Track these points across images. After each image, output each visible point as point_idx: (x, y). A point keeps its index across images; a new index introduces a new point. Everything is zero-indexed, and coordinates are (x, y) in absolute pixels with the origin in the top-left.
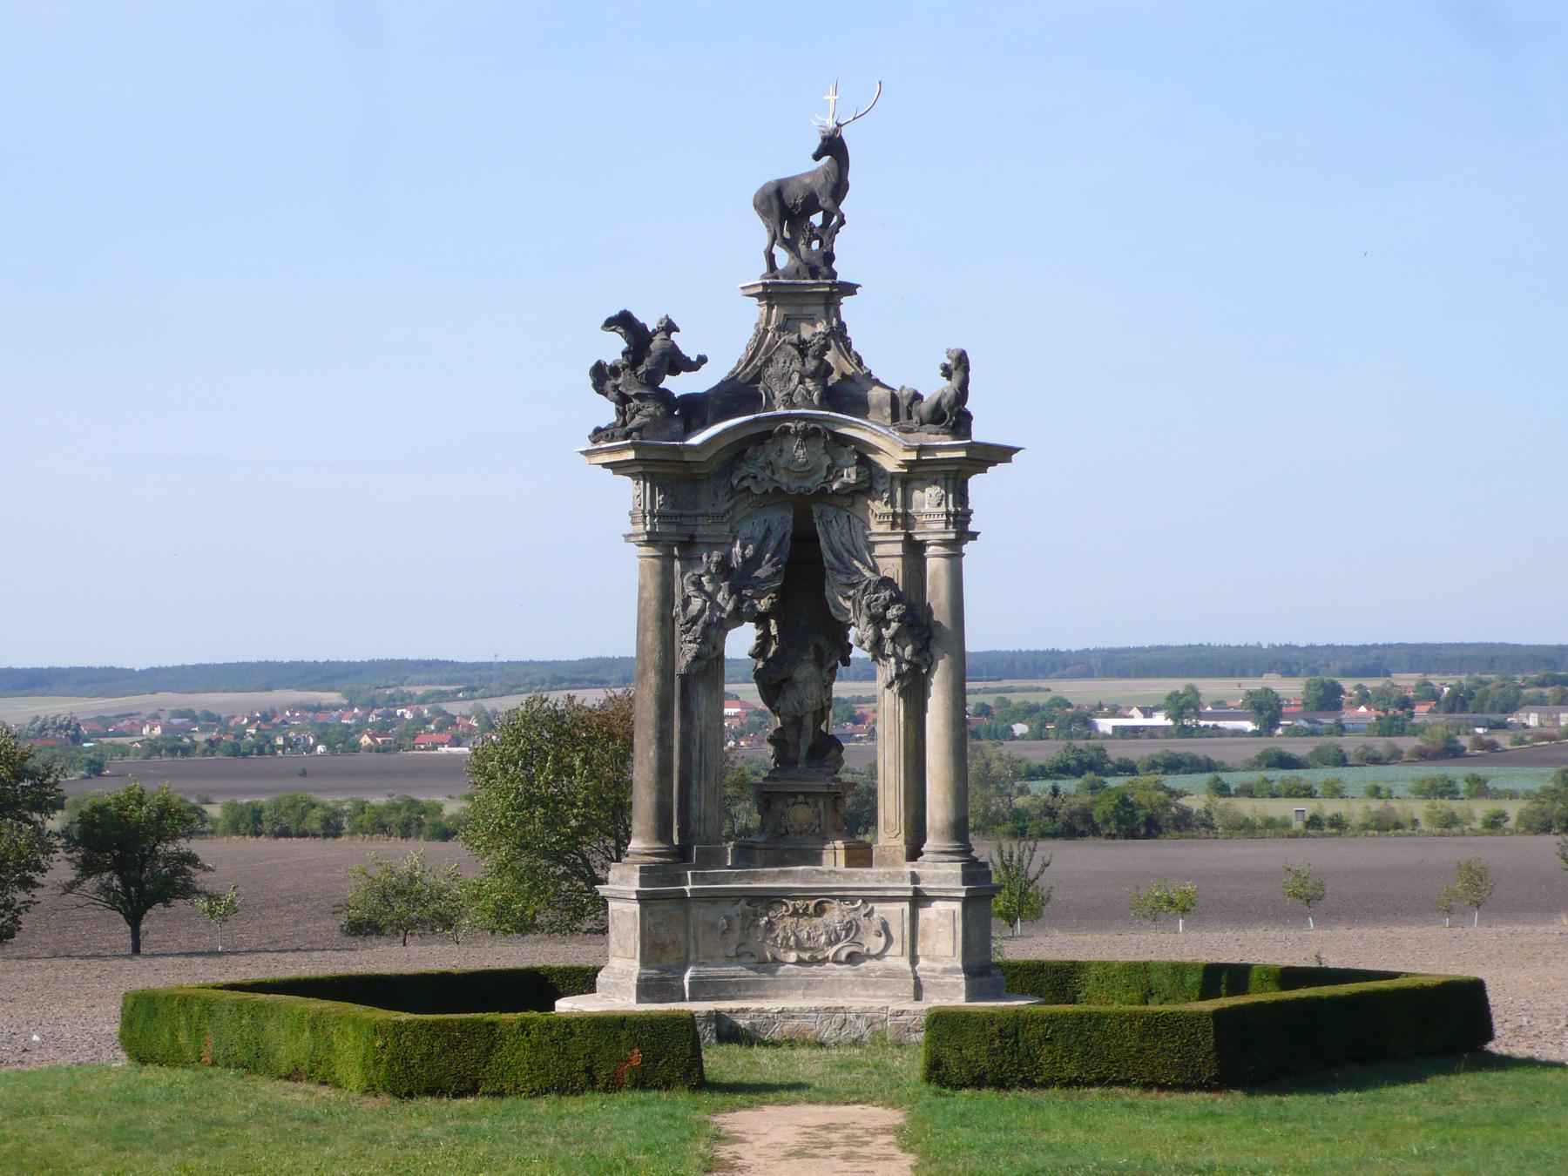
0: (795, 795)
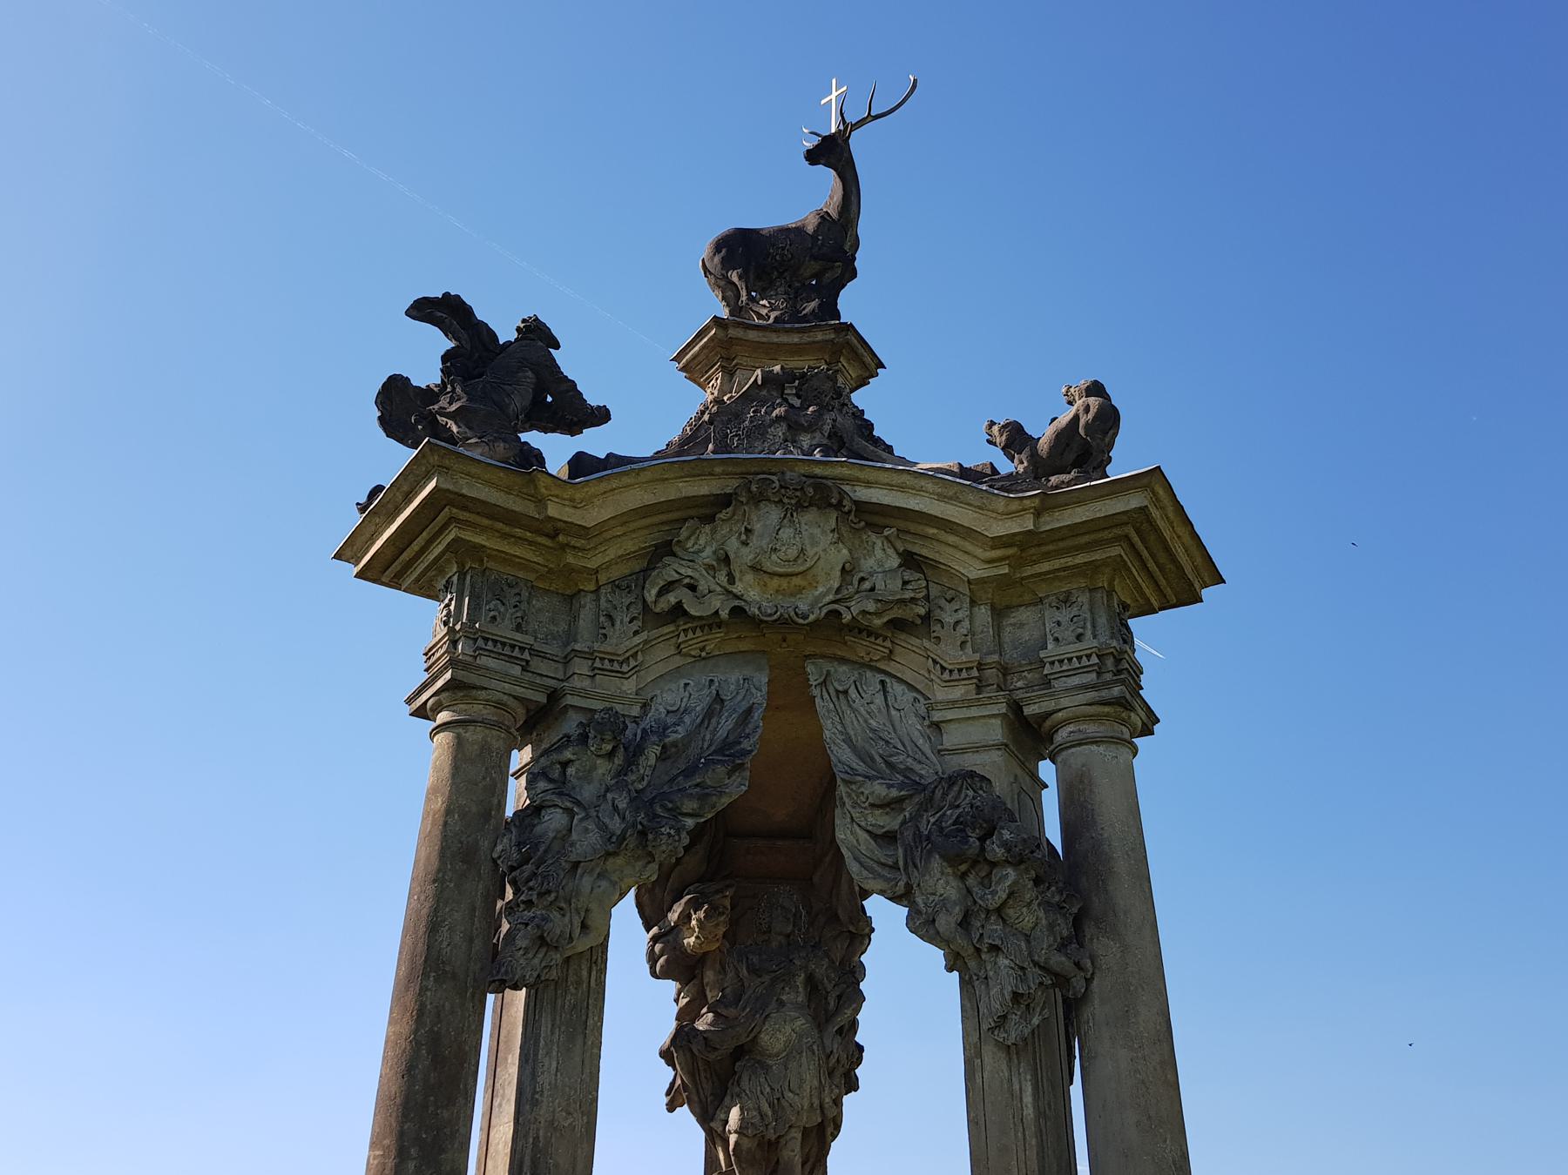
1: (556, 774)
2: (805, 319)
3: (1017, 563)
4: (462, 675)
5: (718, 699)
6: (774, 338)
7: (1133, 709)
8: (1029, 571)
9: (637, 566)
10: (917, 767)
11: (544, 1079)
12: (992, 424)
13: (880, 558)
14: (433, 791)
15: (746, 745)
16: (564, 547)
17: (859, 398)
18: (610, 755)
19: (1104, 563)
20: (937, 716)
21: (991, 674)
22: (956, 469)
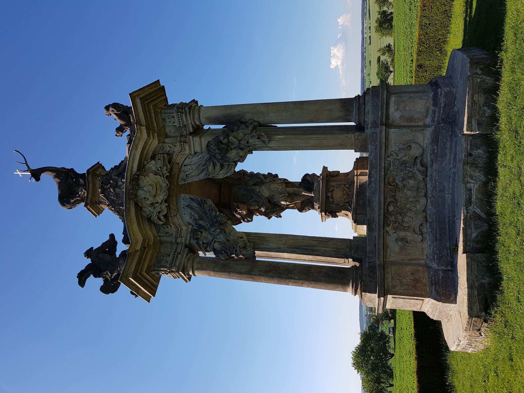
0: (327, 197)
1: (205, 245)
2: (85, 182)
3: (154, 131)
4: (181, 269)
5: (188, 206)
6: (90, 191)
7: (191, 106)
8: (156, 128)
9: (153, 227)
10: (205, 158)
11: (275, 246)
12: (116, 135)
13: (152, 165)
14: (209, 275)
15: (199, 200)
16: (148, 245)
17: (108, 169)
18: (201, 232)
19: (154, 109)
20: (193, 153)
21: (183, 139)
22: (129, 145)
